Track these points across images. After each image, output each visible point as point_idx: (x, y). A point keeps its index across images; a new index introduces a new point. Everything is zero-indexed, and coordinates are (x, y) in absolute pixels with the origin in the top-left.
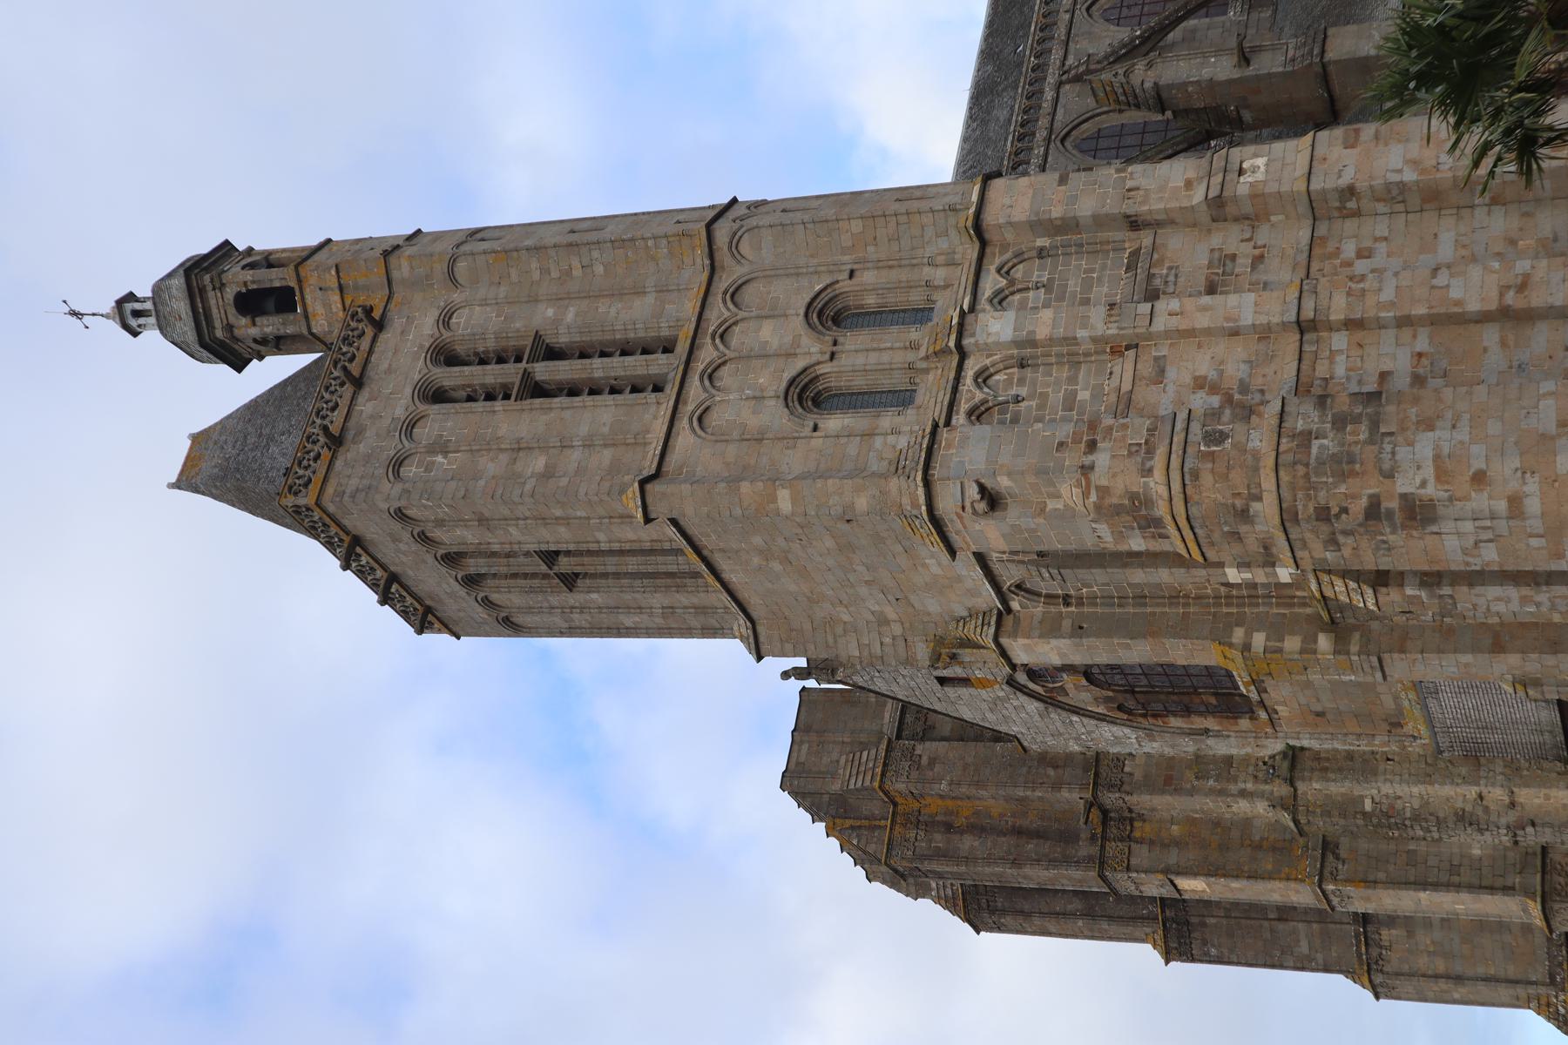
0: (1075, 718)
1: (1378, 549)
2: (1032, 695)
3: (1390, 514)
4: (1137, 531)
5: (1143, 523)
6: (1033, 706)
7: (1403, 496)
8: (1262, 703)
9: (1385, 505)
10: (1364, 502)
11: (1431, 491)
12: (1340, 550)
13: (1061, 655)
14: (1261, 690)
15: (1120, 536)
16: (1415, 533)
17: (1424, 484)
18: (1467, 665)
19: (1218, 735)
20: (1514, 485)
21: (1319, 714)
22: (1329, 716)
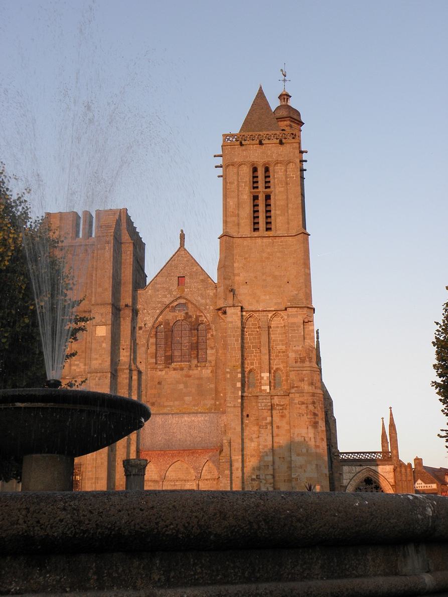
0: (158, 311)
1: (300, 413)
2: (173, 302)
3: (315, 418)
4: (298, 356)
5: (303, 359)
6: (167, 301)
7: (318, 422)
8: (169, 368)
9: (317, 417)
10: (317, 412)
11: (320, 428)
12: (299, 404)
13: (232, 322)
14: (175, 369)
15: (296, 352)
16: (307, 423)
17: (321, 427)
18: (235, 429)
19: (147, 352)
20: (321, 447)
21: (159, 383)
22: (158, 386)
